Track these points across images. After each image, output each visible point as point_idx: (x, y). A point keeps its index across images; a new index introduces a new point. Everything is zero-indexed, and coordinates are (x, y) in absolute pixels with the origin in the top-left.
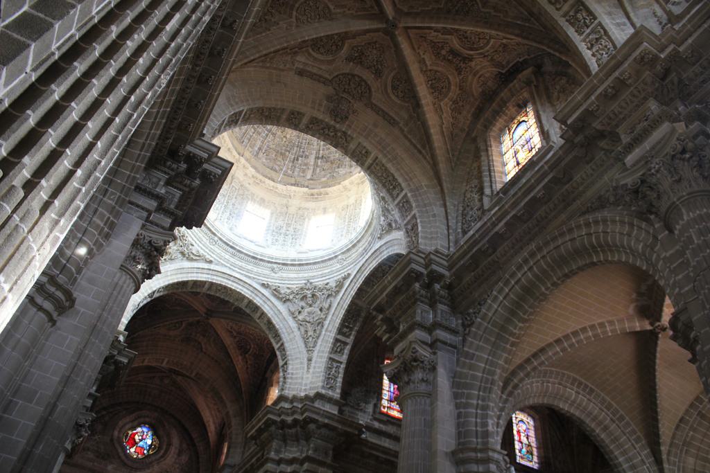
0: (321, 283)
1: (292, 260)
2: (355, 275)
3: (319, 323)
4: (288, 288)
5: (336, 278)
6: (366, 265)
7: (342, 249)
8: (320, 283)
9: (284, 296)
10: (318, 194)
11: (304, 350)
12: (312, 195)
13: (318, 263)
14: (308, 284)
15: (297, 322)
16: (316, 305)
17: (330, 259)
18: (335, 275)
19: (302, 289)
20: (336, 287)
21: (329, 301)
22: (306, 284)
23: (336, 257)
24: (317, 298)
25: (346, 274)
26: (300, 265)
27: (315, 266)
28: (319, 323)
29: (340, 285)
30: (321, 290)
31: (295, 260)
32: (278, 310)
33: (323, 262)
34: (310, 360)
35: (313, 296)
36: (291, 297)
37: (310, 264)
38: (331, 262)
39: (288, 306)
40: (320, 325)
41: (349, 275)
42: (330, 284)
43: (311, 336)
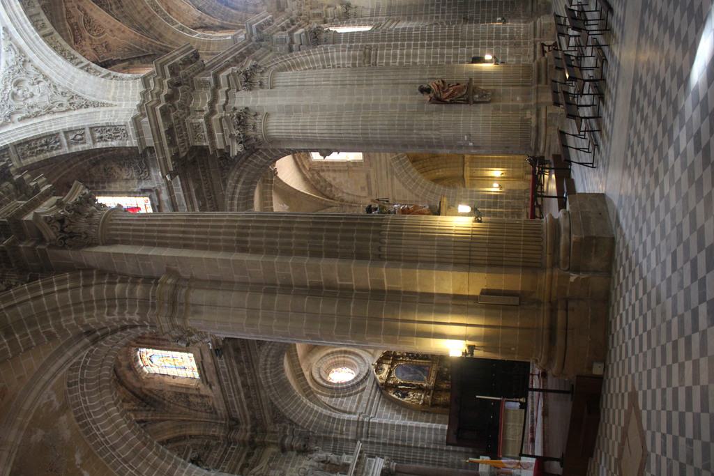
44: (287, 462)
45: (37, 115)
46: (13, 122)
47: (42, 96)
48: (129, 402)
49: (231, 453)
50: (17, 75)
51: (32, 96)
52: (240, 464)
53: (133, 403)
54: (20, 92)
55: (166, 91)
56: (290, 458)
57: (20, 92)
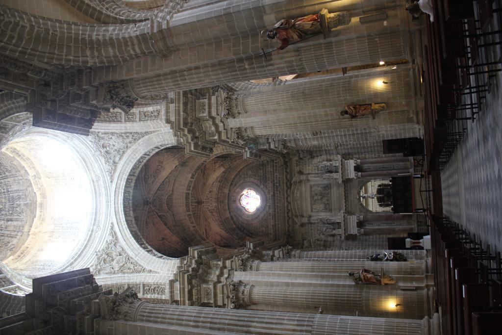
0: (104, 245)
1: (72, 258)
2: (116, 218)
3: (128, 258)
5: (108, 234)
6: (116, 205)
7: (91, 223)
8: (102, 247)
9: (95, 271)
10: (22, 253)
11: (141, 274)
12: (19, 256)
13: (87, 245)
14: (98, 253)
15: (118, 273)
16: (114, 257)
17: (91, 236)
18: (104, 235)
19: (98, 259)
20: (113, 237)
21: (118, 247)
22: (97, 255)
23: (92, 231)
24: (111, 253)
25: (110, 225)
26: (80, 255)
28: (128, 258)
29: (114, 234)
30: (107, 248)
31: (74, 257)
32: (103, 278)
33: (88, 241)
34: (150, 271)
35: (107, 255)
36: (99, 267)
37: (83, 250)
38: (93, 236)
39: (103, 273)
40: (130, 259)
41: (112, 223)
42: (108, 241)
43: (134, 267)
44: (306, 164)
45: (124, 152)
46: (118, 163)
47: (118, 143)
48: (217, 162)
49: (276, 166)
50: (100, 143)
51: (114, 146)
52: (285, 175)
53: (219, 161)
54: (108, 149)
55: (189, 136)
56: (305, 161)
57: (108, 149)
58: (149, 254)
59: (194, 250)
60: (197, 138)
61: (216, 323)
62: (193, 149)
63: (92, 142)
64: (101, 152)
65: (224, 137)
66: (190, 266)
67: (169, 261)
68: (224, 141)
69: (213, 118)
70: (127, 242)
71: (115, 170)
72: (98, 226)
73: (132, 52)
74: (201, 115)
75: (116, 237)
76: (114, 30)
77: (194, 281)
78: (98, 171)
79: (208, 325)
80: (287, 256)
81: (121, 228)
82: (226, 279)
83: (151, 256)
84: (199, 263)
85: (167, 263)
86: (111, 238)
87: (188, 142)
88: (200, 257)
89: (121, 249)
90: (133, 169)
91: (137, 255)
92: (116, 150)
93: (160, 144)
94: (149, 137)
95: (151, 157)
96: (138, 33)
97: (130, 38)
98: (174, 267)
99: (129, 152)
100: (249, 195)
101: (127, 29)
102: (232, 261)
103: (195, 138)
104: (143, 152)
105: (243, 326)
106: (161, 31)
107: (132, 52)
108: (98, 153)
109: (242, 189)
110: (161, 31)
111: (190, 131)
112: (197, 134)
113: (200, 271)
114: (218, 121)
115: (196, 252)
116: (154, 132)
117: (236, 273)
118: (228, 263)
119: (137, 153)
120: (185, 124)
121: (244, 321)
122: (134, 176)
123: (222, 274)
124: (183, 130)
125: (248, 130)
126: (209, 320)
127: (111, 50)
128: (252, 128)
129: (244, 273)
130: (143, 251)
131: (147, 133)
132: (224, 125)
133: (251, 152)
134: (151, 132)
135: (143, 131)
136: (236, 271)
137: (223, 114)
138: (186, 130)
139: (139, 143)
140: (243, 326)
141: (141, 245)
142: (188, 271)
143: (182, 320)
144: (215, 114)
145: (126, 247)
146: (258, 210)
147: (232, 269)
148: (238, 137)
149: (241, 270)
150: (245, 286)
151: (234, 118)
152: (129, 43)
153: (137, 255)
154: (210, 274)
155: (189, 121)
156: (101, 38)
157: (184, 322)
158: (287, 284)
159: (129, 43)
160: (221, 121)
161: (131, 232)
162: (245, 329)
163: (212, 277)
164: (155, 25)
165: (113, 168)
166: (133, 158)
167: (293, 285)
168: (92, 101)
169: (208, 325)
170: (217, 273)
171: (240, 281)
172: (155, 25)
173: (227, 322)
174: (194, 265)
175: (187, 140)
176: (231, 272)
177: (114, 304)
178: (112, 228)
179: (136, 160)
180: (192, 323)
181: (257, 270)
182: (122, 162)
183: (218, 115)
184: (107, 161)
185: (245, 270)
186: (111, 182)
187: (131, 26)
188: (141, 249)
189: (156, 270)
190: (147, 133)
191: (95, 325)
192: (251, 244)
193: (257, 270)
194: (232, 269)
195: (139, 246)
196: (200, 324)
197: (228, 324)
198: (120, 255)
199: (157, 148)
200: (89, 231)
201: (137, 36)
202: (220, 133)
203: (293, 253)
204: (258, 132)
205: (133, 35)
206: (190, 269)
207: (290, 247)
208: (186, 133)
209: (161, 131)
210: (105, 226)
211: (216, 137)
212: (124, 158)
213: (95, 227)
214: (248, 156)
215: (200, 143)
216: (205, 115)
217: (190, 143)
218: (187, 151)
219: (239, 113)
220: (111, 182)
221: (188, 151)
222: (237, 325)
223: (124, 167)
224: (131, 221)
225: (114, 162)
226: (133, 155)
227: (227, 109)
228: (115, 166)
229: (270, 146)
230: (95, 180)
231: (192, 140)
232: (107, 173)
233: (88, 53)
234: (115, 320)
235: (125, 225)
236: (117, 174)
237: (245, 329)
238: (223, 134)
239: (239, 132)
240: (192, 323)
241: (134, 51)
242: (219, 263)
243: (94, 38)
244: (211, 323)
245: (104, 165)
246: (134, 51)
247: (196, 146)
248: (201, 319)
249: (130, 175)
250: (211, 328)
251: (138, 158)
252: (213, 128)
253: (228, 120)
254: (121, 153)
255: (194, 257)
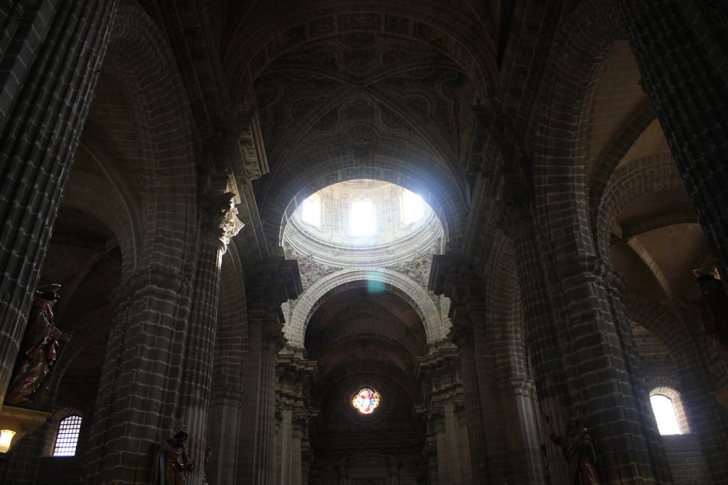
0: (319, 262)
1: (305, 231)
4: (297, 253)
19: (305, 259)
20: (327, 271)
22: (309, 256)
23: (333, 248)
25: (340, 267)
27: (316, 245)
30: (315, 266)
38: (328, 249)
41: (342, 269)
51: (426, 272)
55: (435, 362)
58: (308, 311)
59: (314, 366)
60: (434, 369)
61: (263, 436)
62: (421, 364)
63: (429, 250)
64: (418, 259)
65: (434, 398)
66: (298, 363)
67: (301, 335)
68: (430, 398)
69: (454, 388)
70: (322, 286)
71: (399, 271)
72: (338, 254)
73: (497, 356)
74: (457, 375)
75: (327, 274)
76: (517, 338)
77: (282, 369)
78: (398, 254)
79: (262, 430)
80: (305, 458)
81: (336, 279)
82: (285, 403)
83: (307, 314)
84: (301, 372)
85: (299, 333)
86: (326, 269)
87: (429, 359)
88: (307, 372)
89: (314, 280)
90: (401, 291)
91: (307, 297)
92: (421, 274)
93: (428, 324)
94: (435, 311)
95: (414, 310)
96: (513, 364)
97: (509, 356)
98: (295, 341)
99: (420, 287)
100: (373, 400)
101: (518, 351)
102: (302, 407)
103: (433, 366)
104: (419, 304)
105: (262, 461)
106: (513, 387)
107: (497, 356)
108: (417, 256)
109: (380, 392)
110: (513, 387)
111: (440, 363)
112: (437, 369)
113: (292, 374)
114: (451, 393)
115: (312, 368)
116: (441, 317)
117: (290, 412)
118: (301, 403)
119: (419, 296)
120: (448, 359)
121: (266, 462)
122: (394, 290)
123: (289, 397)
124: (441, 356)
125: (441, 426)
126: (266, 430)
127: (498, 336)
128: (444, 430)
129: (290, 422)
130: (313, 304)
131: (439, 309)
132: (447, 399)
133: (422, 413)
134: (440, 314)
135: (441, 305)
136: (293, 413)
137: (457, 401)
138: (441, 359)
139: (428, 299)
140: (262, 461)
141: (319, 301)
142: (293, 362)
143: (265, 404)
144: (459, 392)
145: (316, 285)
146: (356, 410)
147: (294, 407)
148: (433, 415)
149: (293, 418)
150: (277, 425)
151: (455, 412)
152: (504, 354)
153: (307, 297)
154: (289, 385)
155: (451, 363)
156: (509, 329)
157: (263, 406)
158: (279, 471)
159: (504, 354)
160: (450, 398)
161: (333, 290)
162: (260, 463)
163: (287, 386)
164: (518, 383)
165: (402, 270)
166: (413, 291)
167: (279, 477)
168: (457, 311)
169: (262, 430)
170: (291, 392)
171: (282, 419)
172: (518, 383)
173: (265, 447)
174: (298, 367)
175: (431, 359)
176: (291, 407)
177: (276, 337)
178: (337, 269)
179: (411, 296)
180: (262, 414)
181: (294, 436)
182: (408, 279)
183: (458, 394)
184: (408, 264)
185: (293, 422)
186: (387, 268)
187: (521, 354)
188: (315, 302)
189: (292, 320)
190: (439, 309)
191: (258, 319)
192: (316, 414)
193: (294, 436)
194: (294, 407)
195: (317, 299)
196: (262, 422)
197: (263, 448)
198: (308, 280)
199: (424, 319)
200: (334, 244)
201: (509, 363)
202: (438, 394)
203: (307, 464)
204: (440, 437)
205: (511, 359)
206: (295, 364)
207: (312, 459)
208: (438, 359)
209: (442, 326)
210: (339, 261)
211: (434, 389)
212: (412, 282)
213: (338, 250)
214: (418, 411)
215: (428, 371)
216: (458, 380)
217: (427, 361)
218: (419, 358)
219: (459, 418)
220: (387, 268)
221: (418, 360)
222: (262, 455)
223: (402, 282)
224: (344, 288)
225: (408, 271)
226: (415, 291)
227: (463, 406)
228: (403, 273)
229: (429, 436)
230: (388, 249)
231: (431, 364)
232: (395, 263)
233: (496, 316)
234: (263, 339)
235: (339, 283)
236: (395, 274)
237: (260, 463)
238: (438, 397)
239: (440, 416)
240: (262, 414)
241: (499, 358)
242: (300, 393)
243: (509, 323)
244: (264, 431)
245: (405, 261)
246: (499, 358)
247: (424, 367)
248: (266, 422)
249: (394, 287)
250: (259, 432)
251: (413, 298)
252: (443, 387)
253: (452, 405)
254: (418, 279)
255: (306, 367)
